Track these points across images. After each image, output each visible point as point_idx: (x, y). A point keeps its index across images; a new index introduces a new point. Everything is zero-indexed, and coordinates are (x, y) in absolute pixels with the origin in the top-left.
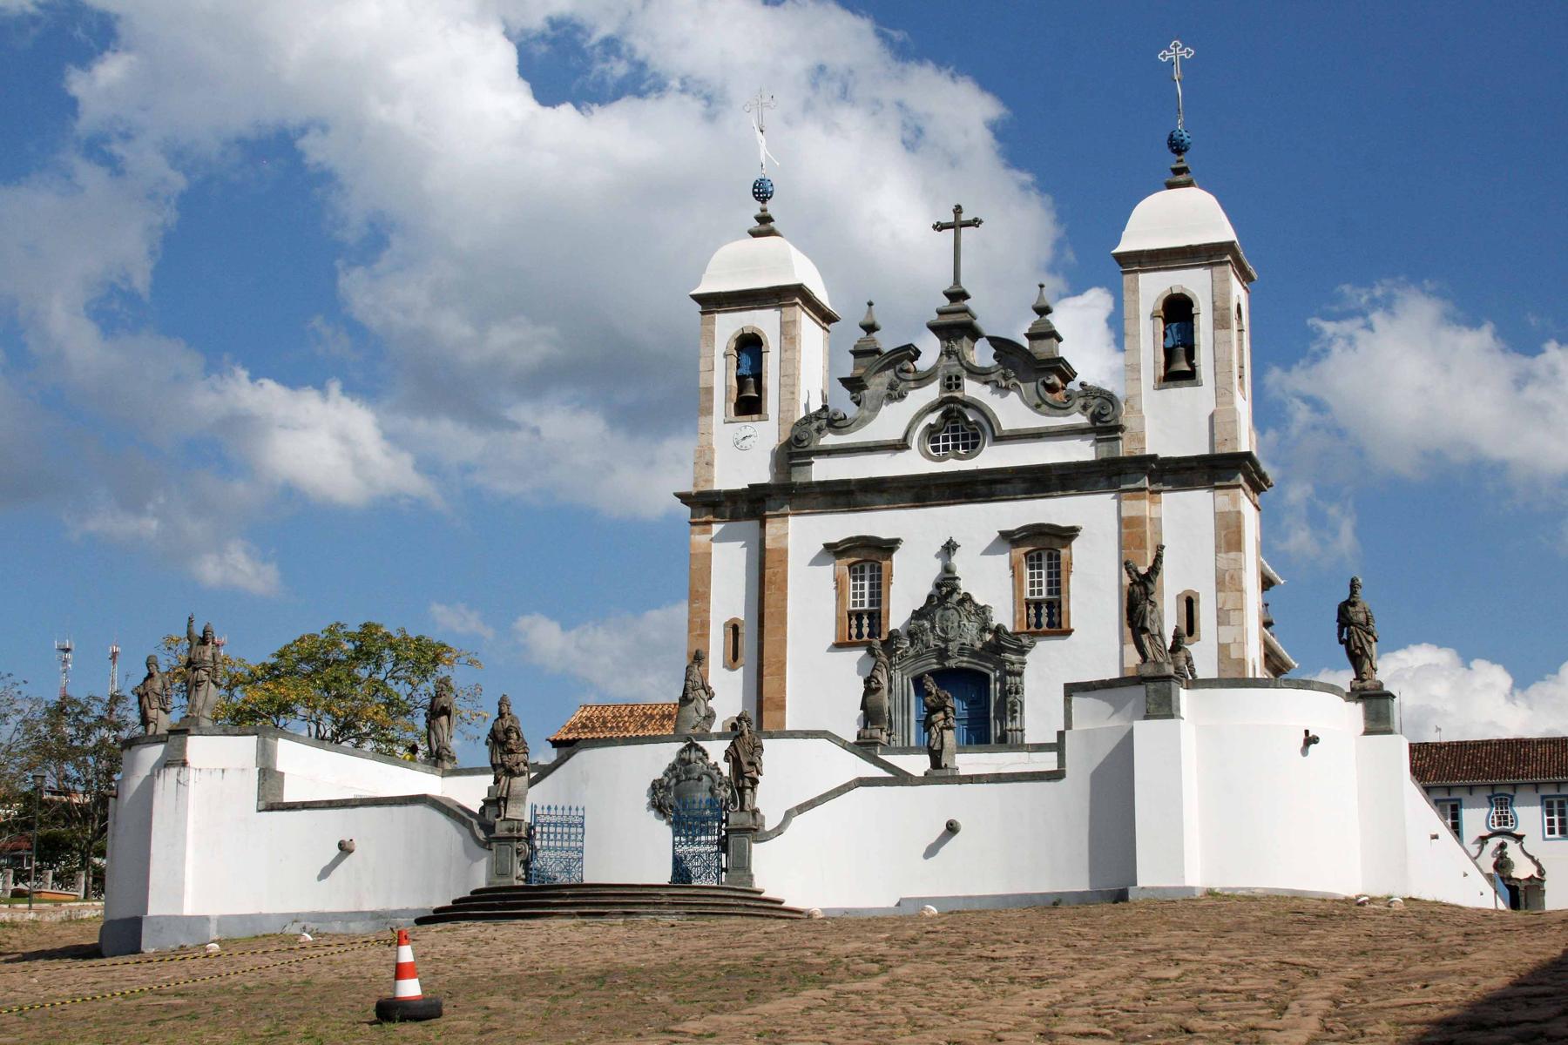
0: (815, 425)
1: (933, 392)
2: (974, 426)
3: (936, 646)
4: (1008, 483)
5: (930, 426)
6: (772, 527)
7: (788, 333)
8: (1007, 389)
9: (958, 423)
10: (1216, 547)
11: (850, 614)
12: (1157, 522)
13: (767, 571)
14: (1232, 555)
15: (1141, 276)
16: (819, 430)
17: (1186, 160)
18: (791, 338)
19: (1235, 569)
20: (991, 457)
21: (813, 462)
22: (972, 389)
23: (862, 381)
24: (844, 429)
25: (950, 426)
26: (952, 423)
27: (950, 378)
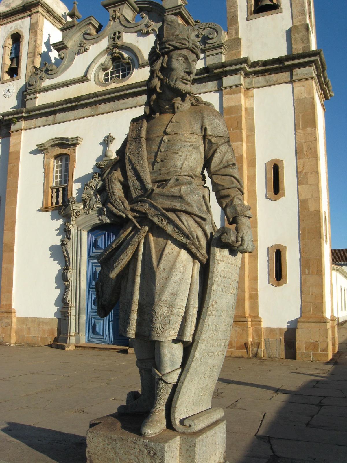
2: (128, 61)
3: (97, 207)
6: (13, 139)
7: (34, 28)
9: (120, 62)
10: (295, 125)
12: (250, 112)
13: (9, 165)
14: (309, 130)
16: (41, 78)
18: (34, 32)
19: (311, 141)
21: (36, 98)
23: (64, 44)
24: (55, 75)
25: (115, 64)
26: (116, 63)
27: (115, 34)
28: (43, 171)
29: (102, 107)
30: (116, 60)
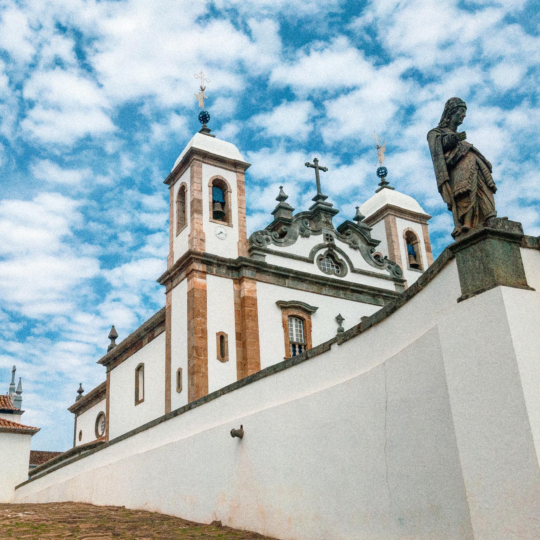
0: (265, 236)
1: (319, 239)
4: (361, 294)
5: (321, 254)
6: (247, 285)
8: (355, 249)
9: (329, 258)
11: (291, 342)
15: (396, 218)
16: (268, 240)
17: (387, 179)
20: (350, 278)
21: (265, 256)
22: (338, 243)
23: (291, 222)
24: (279, 244)
27: (327, 235)
28: (281, 324)
29: (325, 290)
30: (330, 255)
